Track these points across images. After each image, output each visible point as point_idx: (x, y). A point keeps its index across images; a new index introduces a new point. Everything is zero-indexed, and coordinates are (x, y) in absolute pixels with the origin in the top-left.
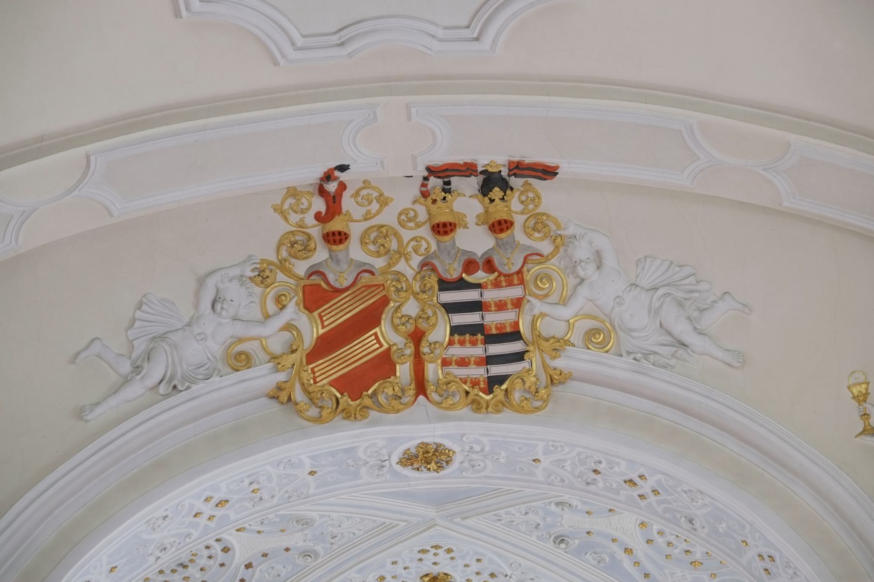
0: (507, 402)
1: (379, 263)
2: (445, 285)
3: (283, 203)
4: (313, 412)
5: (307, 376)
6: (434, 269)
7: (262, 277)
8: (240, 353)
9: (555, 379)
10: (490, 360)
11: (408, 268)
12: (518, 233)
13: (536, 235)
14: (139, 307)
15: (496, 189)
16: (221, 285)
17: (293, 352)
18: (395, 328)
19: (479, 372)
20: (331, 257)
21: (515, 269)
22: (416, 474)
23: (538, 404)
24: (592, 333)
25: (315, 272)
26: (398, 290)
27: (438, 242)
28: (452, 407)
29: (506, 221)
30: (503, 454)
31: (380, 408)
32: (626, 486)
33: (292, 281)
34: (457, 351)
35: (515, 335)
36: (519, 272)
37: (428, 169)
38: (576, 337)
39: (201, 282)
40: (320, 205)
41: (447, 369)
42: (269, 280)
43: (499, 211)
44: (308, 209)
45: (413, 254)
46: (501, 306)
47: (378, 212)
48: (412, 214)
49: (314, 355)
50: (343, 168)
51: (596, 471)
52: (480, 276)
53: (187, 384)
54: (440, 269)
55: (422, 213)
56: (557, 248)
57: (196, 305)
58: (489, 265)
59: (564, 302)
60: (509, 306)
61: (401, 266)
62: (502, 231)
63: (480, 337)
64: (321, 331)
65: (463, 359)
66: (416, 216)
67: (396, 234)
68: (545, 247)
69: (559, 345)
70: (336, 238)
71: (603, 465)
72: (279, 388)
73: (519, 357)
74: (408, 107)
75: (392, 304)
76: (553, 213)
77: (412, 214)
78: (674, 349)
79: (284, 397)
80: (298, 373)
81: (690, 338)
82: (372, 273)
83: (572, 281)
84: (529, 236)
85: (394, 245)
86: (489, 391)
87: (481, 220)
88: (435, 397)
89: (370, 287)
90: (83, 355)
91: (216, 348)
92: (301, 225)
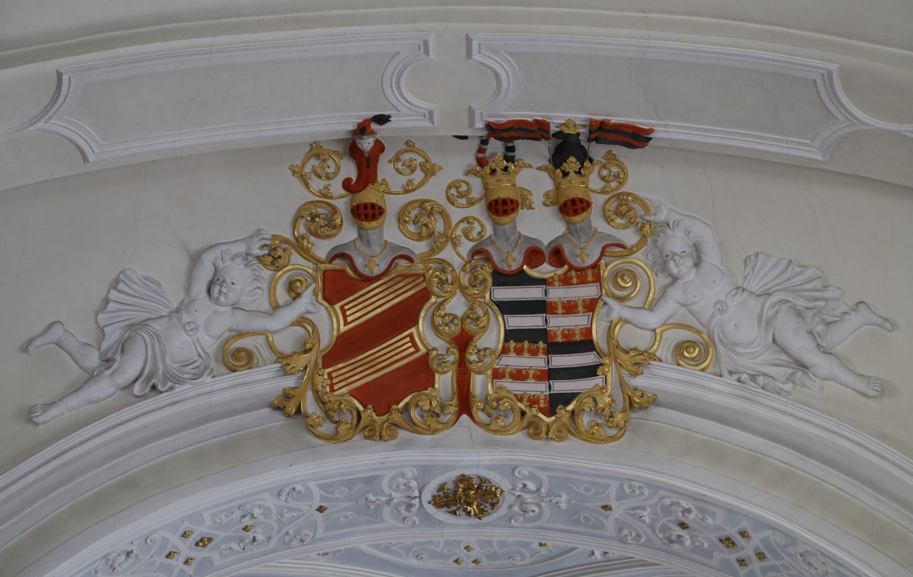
0: (572, 428)
1: (420, 248)
2: (502, 278)
3: (304, 164)
4: (327, 428)
5: (322, 381)
6: (489, 259)
8: (239, 350)
10: (553, 374)
12: (596, 220)
13: (619, 221)
15: (572, 159)
16: (220, 264)
18: (436, 328)
19: (539, 388)
21: (590, 262)
23: (613, 432)
25: (340, 254)
26: (442, 282)
27: (495, 224)
28: (503, 430)
29: (581, 201)
30: (564, 497)
31: (413, 427)
34: (512, 361)
35: (587, 345)
36: (595, 266)
38: (664, 350)
39: (195, 259)
40: (349, 170)
41: (499, 383)
42: (281, 261)
43: (574, 188)
44: (335, 174)
45: (463, 239)
46: (570, 308)
47: (422, 184)
48: (464, 188)
49: (332, 357)
51: (683, 525)
52: (545, 270)
53: (169, 384)
54: (496, 259)
56: (644, 237)
57: (188, 288)
58: (557, 256)
60: (580, 308)
61: (448, 253)
62: (576, 212)
64: (343, 329)
65: (519, 371)
66: (469, 190)
67: (443, 213)
68: (629, 237)
71: (692, 516)
72: (287, 395)
75: (433, 299)
76: (641, 194)
77: (464, 188)
78: (790, 371)
79: (292, 409)
80: (312, 378)
81: (813, 357)
82: (410, 260)
83: (663, 280)
84: (608, 220)
85: (439, 226)
86: (550, 412)
87: (551, 200)
88: (481, 416)
89: (406, 276)
90: (38, 342)
91: (209, 343)
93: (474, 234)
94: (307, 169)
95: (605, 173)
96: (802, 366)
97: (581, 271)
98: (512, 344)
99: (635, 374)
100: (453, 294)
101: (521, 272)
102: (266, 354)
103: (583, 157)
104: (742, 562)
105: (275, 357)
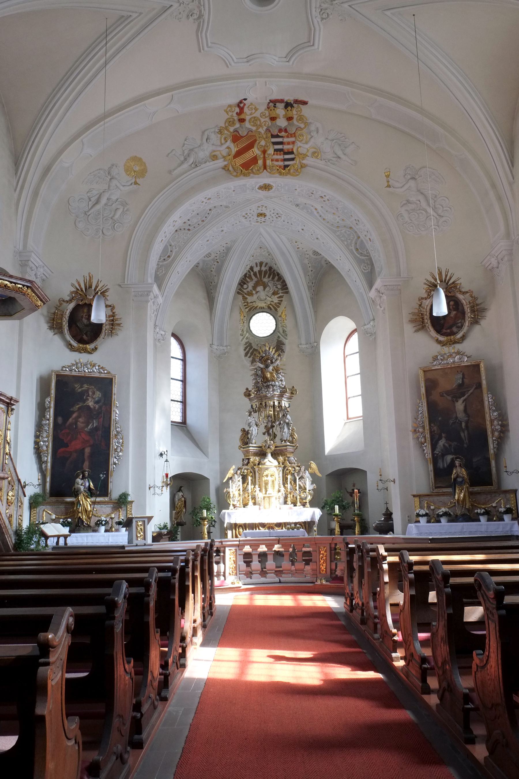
0: (289, 173)
1: (254, 128)
2: (273, 136)
3: (227, 109)
4: (235, 174)
5: (233, 163)
6: (270, 131)
7: (220, 132)
9: (303, 166)
10: (285, 160)
11: (262, 130)
12: (295, 121)
13: (300, 122)
14: (186, 140)
15: (289, 107)
17: (229, 155)
18: (258, 149)
19: (281, 163)
20: (240, 126)
21: (293, 132)
22: (262, 192)
23: (298, 173)
24: (314, 153)
25: (236, 131)
26: (259, 137)
27: (271, 123)
28: (274, 174)
31: (253, 173)
32: (320, 198)
33: (229, 133)
34: (275, 157)
35: (292, 153)
36: (294, 133)
37: (270, 100)
38: (309, 154)
39: (203, 133)
40: (237, 110)
41: (272, 162)
42: (223, 133)
43: (290, 114)
45: (264, 126)
46: (289, 143)
47: (254, 113)
48: (264, 114)
49: (235, 157)
50: (245, 99)
51: (312, 193)
52: (283, 134)
54: (272, 131)
55: (267, 113)
56: (305, 126)
57: (202, 140)
59: (306, 143)
61: (261, 130)
62: (290, 120)
63: (282, 153)
64: (237, 149)
66: (265, 114)
68: (302, 126)
69: (305, 156)
70: (242, 121)
71: (315, 192)
72: (225, 166)
73: (293, 159)
74: (266, 82)
75: (257, 142)
79: (227, 169)
80: (231, 162)
81: (342, 156)
83: (309, 137)
84: (298, 122)
85: (259, 123)
86: (284, 169)
87: (285, 116)
88: (269, 170)
89: (251, 136)
90: (170, 155)
91: (208, 154)
92: (232, 116)
93: (267, 125)
94: (228, 110)
95: (297, 110)
96: (339, 158)
97: (291, 134)
98: (276, 152)
99: (303, 160)
100: (262, 140)
101: (278, 135)
102: (220, 156)
103: (292, 106)
104: (324, 201)
105: (222, 157)
